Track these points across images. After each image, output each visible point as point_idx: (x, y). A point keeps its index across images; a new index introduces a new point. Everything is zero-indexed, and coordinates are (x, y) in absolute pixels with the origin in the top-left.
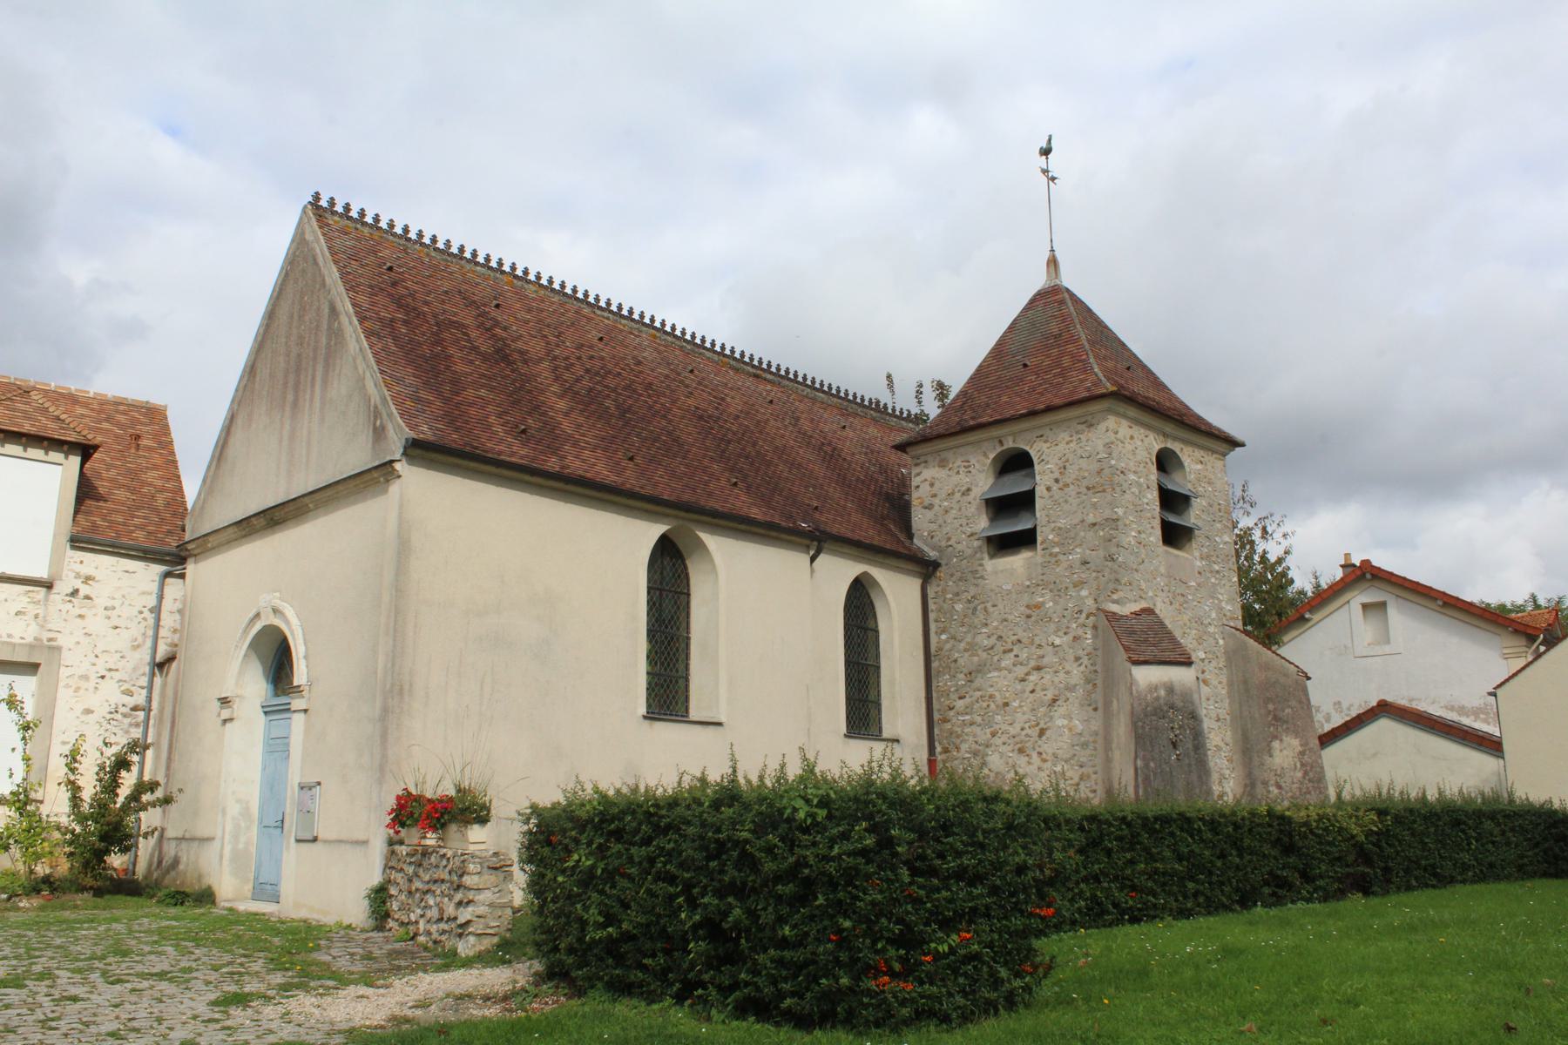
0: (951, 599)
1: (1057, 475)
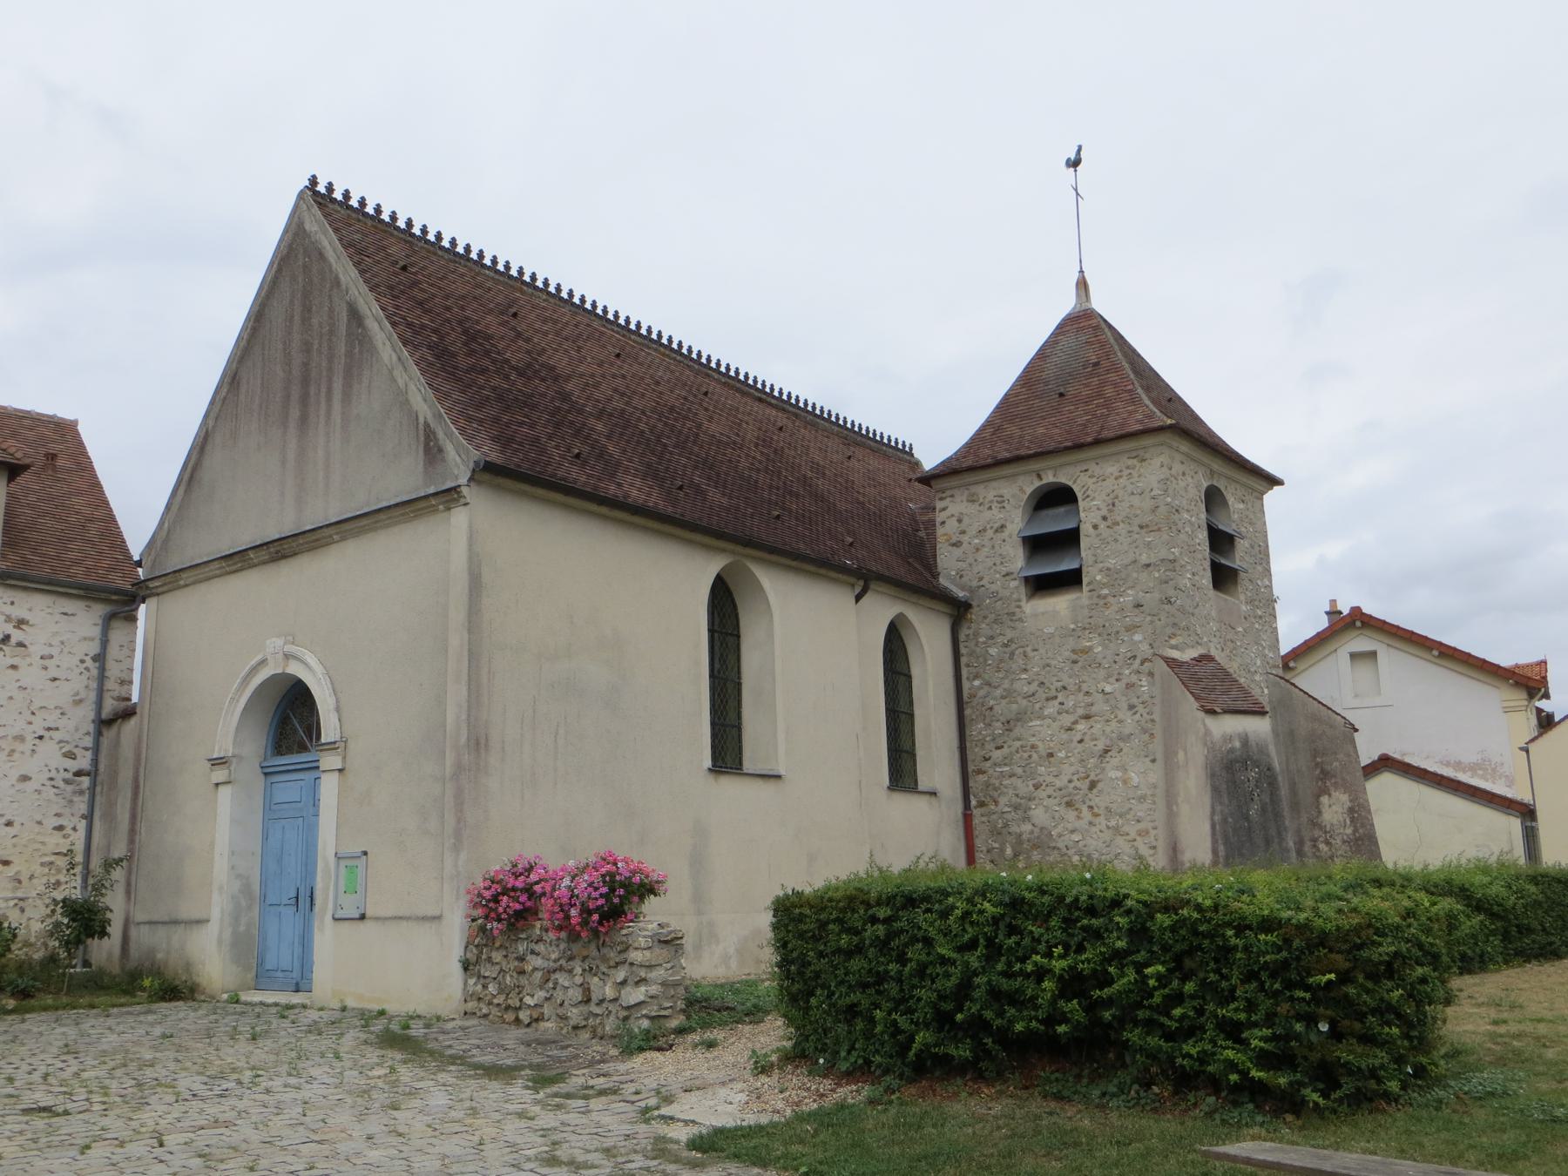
0: (984, 643)
1: (1104, 512)
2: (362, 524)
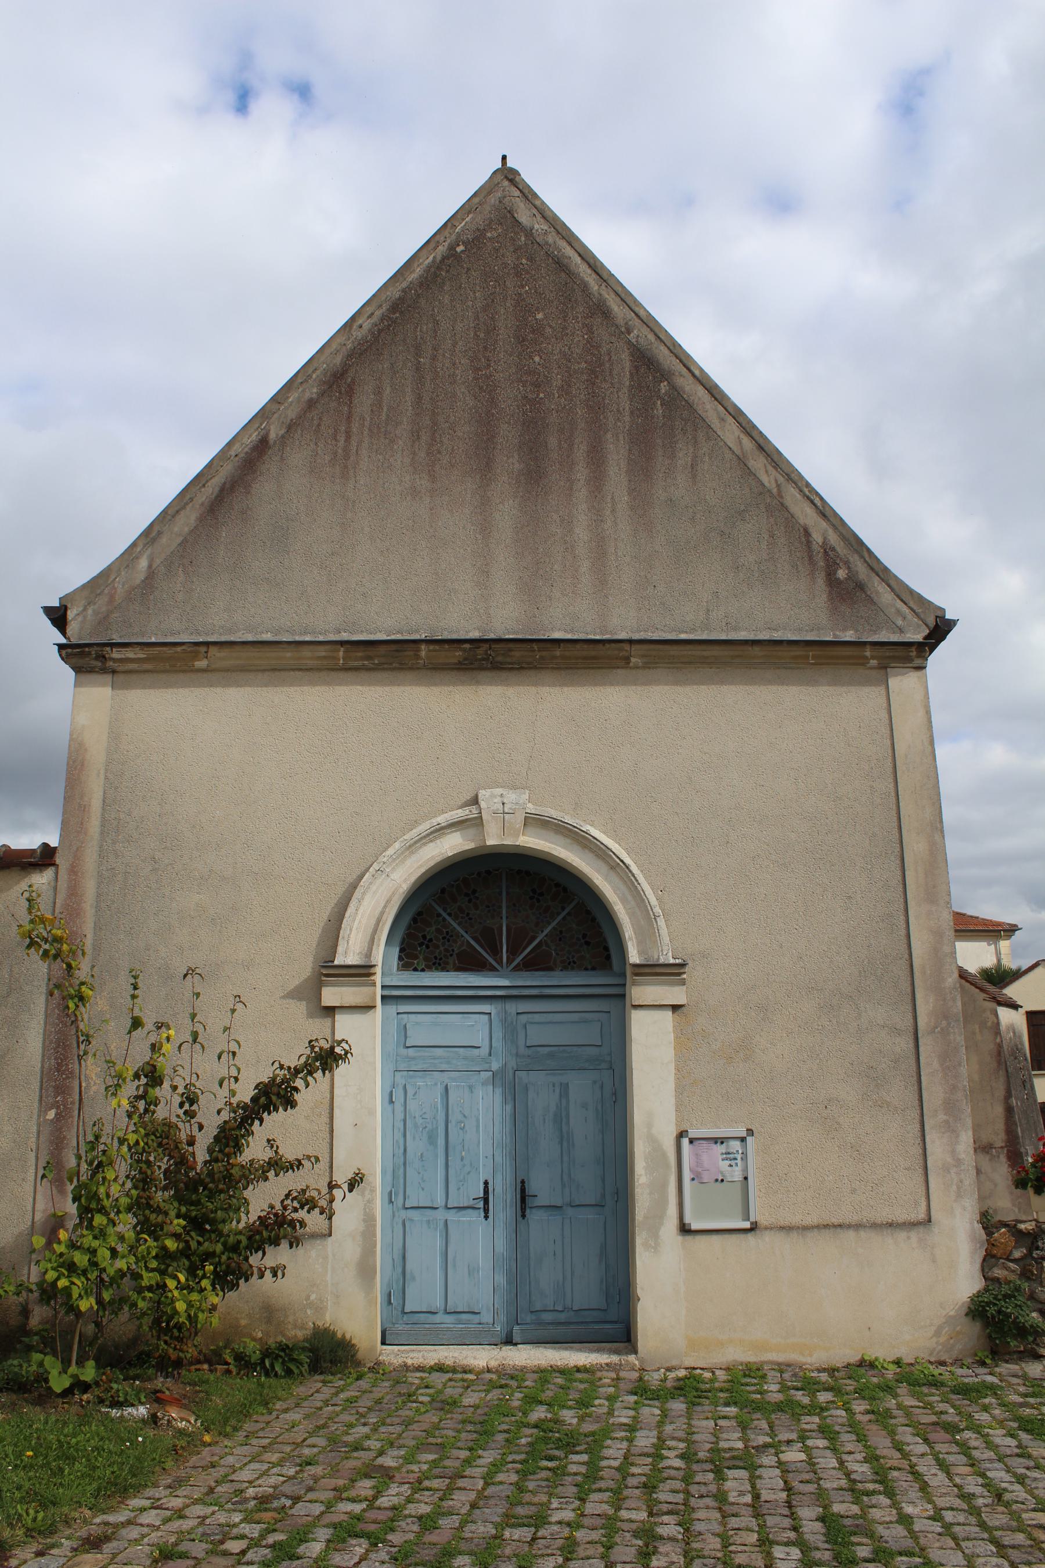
2: (705, 653)
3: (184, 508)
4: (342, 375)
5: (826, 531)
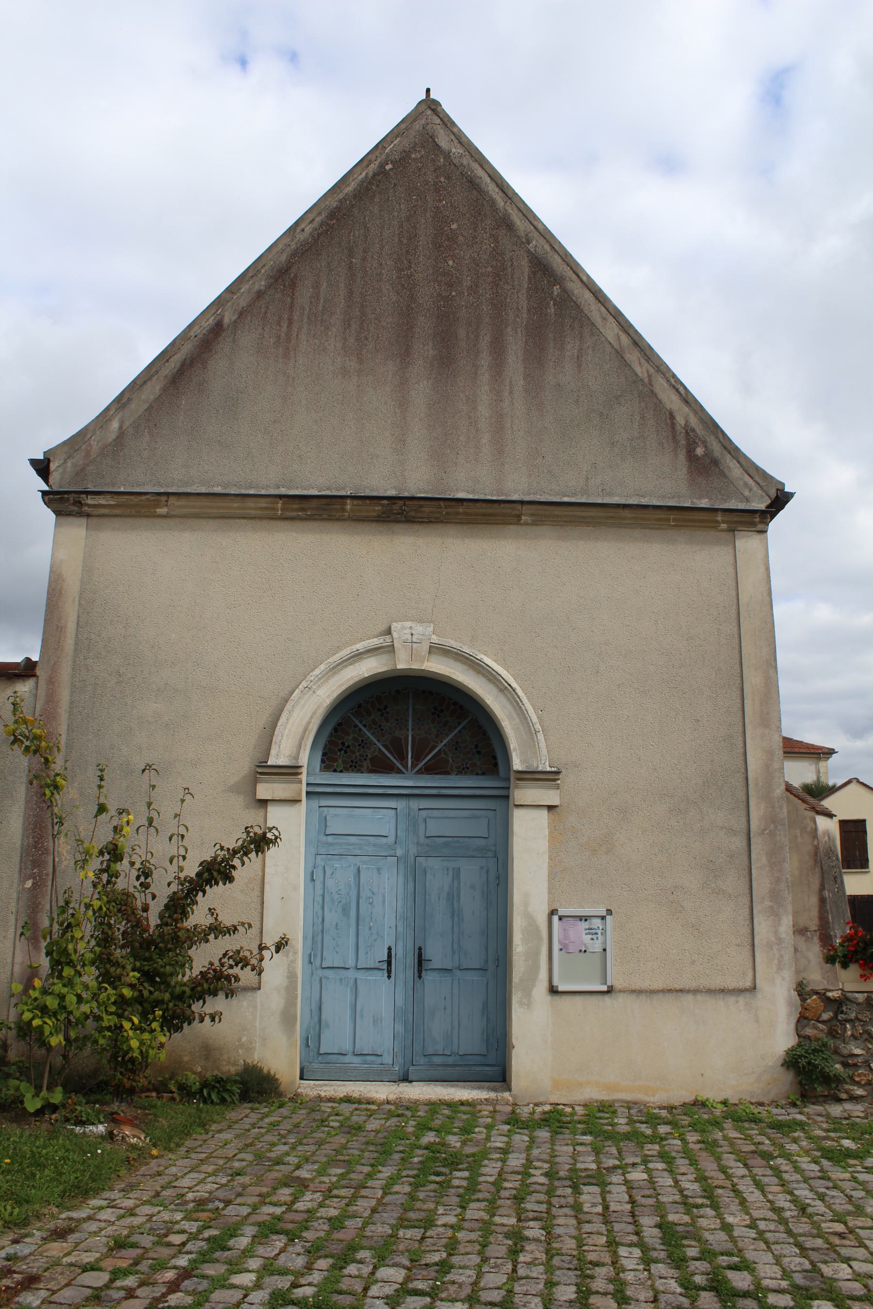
2: (583, 514)
3: (150, 379)
4: (287, 270)
5: (688, 415)
